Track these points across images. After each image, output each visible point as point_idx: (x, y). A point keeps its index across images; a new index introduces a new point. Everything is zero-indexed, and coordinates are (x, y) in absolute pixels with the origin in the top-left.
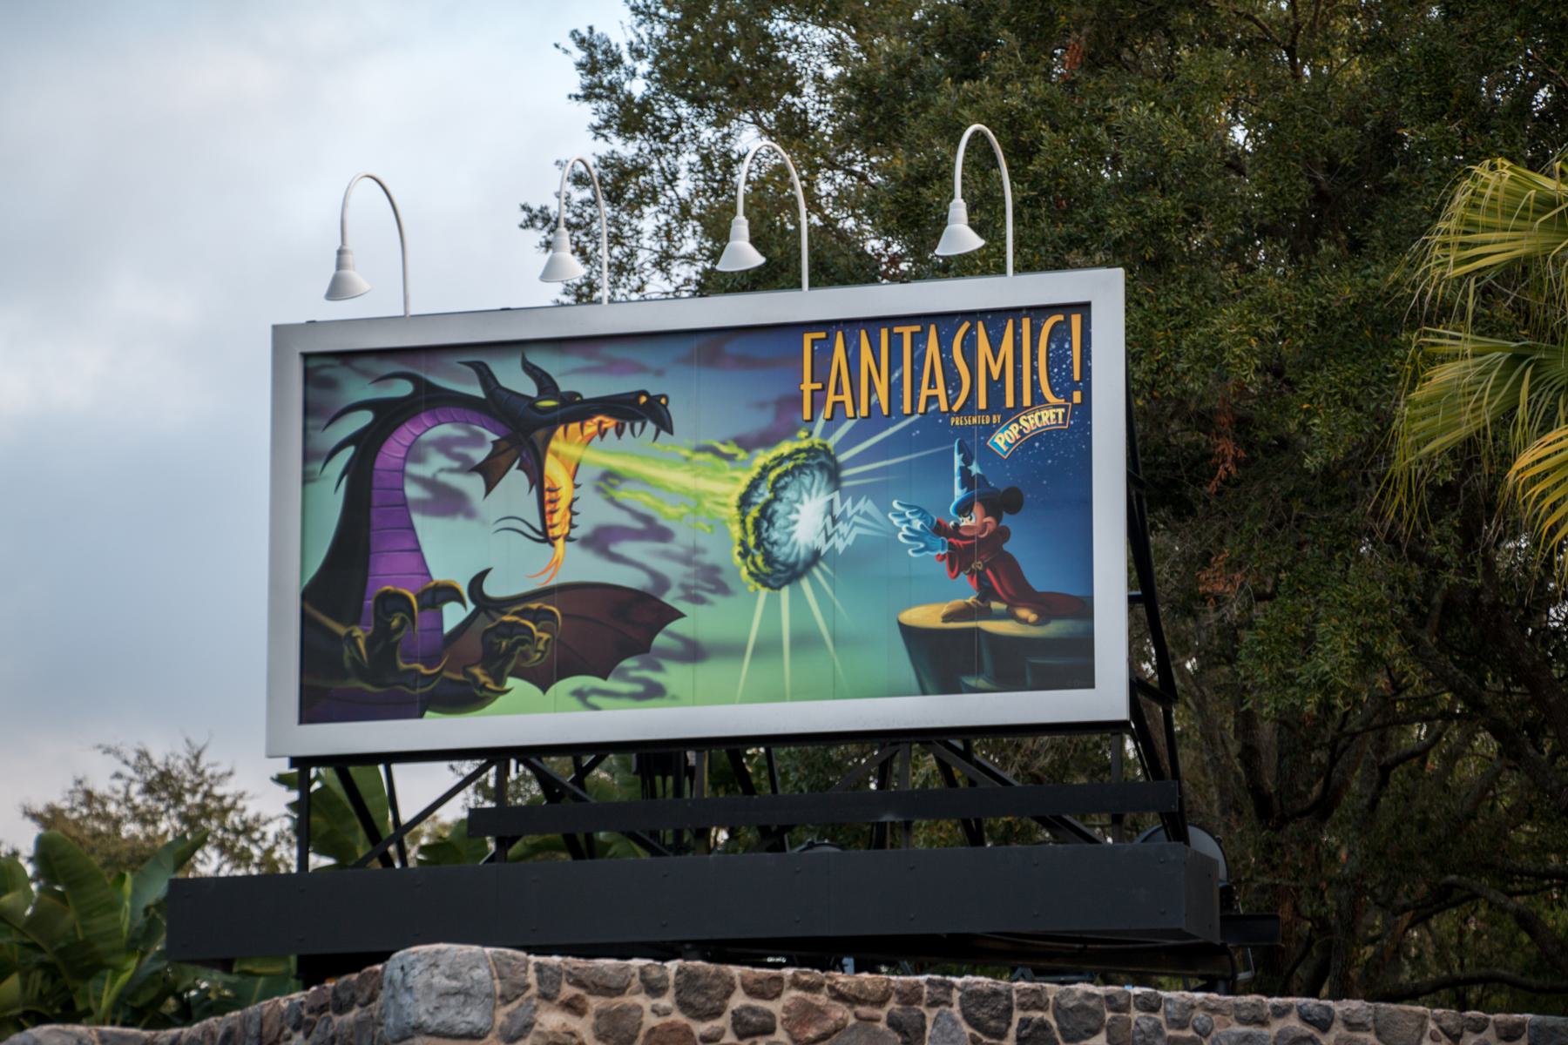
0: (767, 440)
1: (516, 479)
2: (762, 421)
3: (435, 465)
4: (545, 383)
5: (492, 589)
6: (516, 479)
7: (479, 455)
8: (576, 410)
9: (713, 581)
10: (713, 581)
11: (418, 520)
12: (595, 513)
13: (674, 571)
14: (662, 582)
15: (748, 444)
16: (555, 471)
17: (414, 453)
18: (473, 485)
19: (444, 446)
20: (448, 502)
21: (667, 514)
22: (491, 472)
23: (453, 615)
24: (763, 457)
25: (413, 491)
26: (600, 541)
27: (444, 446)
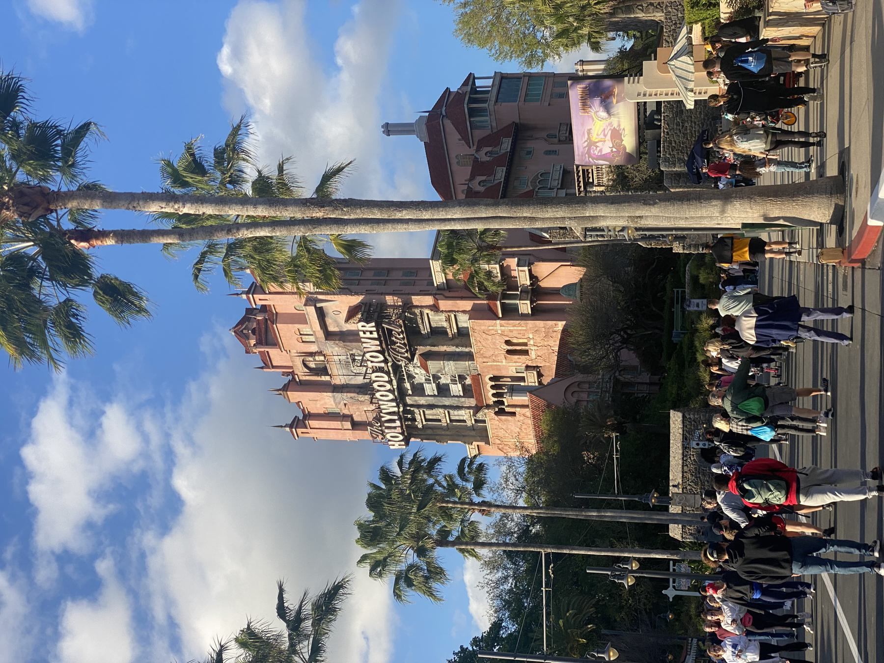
0: (593, 119)
1: (597, 144)
2: (590, 119)
3: (596, 152)
4: (586, 141)
5: (611, 146)
6: (597, 144)
7: (595, 148)
8: (589, 138)
9: (610, 124)
10: (610, 124)
11: (603, 153)
12: (602, 136)
13: (609, 128)
14: (610, 129)
15: (593, 120)
16: (596, 140)
17: (595, 154)
18: (598, 149)
19: (593, 151)
20: (601, 151)
21: (602, 129)
22: (597, 147)
23: (614, 150)
24: (595, 119)
25: (599, 154)
26: (605, 136)
27: (593, 151)
